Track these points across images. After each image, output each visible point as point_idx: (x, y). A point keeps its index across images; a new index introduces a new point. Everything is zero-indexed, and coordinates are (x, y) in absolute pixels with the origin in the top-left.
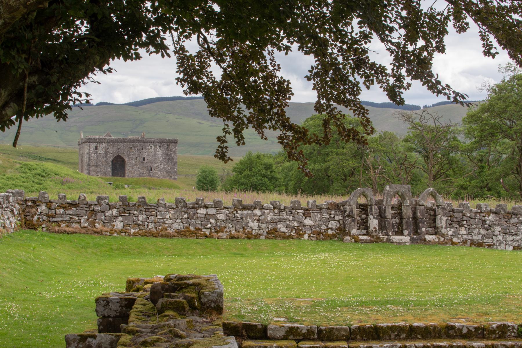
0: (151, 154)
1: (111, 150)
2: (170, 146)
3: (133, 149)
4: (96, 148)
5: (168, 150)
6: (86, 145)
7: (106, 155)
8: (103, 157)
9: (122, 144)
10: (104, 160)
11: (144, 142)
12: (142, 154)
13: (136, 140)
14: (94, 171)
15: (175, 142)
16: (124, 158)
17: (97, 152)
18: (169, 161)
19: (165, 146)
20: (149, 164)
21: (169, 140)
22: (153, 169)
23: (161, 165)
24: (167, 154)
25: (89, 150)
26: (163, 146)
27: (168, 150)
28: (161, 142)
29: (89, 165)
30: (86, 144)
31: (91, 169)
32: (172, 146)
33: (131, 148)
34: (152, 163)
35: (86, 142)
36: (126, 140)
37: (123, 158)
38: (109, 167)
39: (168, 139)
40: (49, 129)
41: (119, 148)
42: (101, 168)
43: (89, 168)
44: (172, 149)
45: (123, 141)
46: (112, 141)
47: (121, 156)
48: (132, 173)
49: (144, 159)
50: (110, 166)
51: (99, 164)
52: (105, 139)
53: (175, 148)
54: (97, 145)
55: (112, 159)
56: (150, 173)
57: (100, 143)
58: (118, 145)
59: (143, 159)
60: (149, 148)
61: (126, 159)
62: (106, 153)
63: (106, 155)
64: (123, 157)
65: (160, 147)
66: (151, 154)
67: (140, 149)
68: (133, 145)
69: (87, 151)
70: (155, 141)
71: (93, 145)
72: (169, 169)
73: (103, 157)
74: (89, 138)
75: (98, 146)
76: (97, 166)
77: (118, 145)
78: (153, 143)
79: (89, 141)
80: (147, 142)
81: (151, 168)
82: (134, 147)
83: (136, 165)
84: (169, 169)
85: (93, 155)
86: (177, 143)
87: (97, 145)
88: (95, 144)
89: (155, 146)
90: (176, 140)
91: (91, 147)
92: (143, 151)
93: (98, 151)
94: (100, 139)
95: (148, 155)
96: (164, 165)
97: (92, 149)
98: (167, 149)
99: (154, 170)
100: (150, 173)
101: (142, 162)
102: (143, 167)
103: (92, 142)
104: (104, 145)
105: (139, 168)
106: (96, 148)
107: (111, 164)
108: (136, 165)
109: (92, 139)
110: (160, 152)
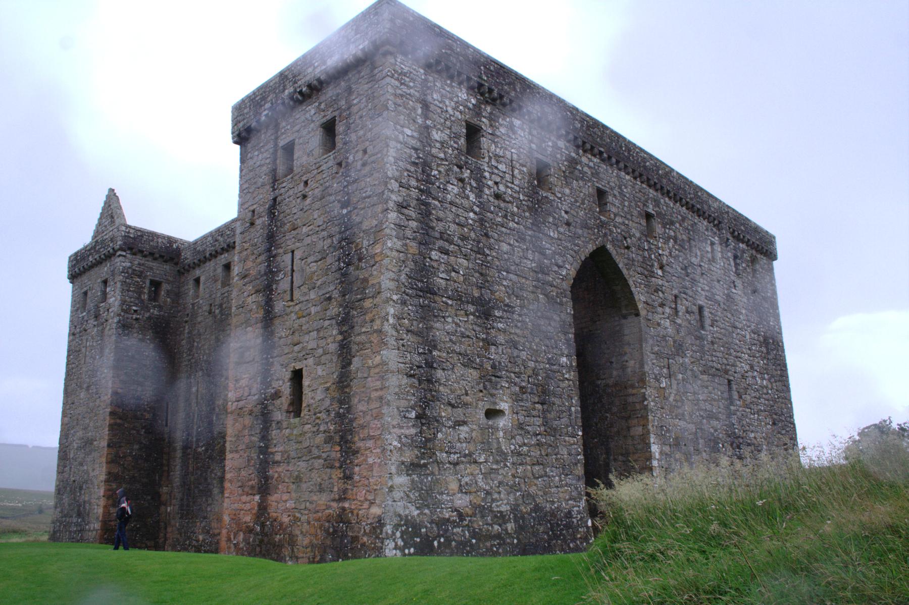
14: (468, 364)
16: (631, 283)
29: (429, 291)
31: (442, 329)
36: (629, 151)
43: (427, 314)
49: (701, 309)
54: (477, 111)
55: (570, 269)
58: (596, 174)
61: (640, 297)
76: (485, 311)
80: (700, 213)
85: (453, 189)
97: (446, 138)
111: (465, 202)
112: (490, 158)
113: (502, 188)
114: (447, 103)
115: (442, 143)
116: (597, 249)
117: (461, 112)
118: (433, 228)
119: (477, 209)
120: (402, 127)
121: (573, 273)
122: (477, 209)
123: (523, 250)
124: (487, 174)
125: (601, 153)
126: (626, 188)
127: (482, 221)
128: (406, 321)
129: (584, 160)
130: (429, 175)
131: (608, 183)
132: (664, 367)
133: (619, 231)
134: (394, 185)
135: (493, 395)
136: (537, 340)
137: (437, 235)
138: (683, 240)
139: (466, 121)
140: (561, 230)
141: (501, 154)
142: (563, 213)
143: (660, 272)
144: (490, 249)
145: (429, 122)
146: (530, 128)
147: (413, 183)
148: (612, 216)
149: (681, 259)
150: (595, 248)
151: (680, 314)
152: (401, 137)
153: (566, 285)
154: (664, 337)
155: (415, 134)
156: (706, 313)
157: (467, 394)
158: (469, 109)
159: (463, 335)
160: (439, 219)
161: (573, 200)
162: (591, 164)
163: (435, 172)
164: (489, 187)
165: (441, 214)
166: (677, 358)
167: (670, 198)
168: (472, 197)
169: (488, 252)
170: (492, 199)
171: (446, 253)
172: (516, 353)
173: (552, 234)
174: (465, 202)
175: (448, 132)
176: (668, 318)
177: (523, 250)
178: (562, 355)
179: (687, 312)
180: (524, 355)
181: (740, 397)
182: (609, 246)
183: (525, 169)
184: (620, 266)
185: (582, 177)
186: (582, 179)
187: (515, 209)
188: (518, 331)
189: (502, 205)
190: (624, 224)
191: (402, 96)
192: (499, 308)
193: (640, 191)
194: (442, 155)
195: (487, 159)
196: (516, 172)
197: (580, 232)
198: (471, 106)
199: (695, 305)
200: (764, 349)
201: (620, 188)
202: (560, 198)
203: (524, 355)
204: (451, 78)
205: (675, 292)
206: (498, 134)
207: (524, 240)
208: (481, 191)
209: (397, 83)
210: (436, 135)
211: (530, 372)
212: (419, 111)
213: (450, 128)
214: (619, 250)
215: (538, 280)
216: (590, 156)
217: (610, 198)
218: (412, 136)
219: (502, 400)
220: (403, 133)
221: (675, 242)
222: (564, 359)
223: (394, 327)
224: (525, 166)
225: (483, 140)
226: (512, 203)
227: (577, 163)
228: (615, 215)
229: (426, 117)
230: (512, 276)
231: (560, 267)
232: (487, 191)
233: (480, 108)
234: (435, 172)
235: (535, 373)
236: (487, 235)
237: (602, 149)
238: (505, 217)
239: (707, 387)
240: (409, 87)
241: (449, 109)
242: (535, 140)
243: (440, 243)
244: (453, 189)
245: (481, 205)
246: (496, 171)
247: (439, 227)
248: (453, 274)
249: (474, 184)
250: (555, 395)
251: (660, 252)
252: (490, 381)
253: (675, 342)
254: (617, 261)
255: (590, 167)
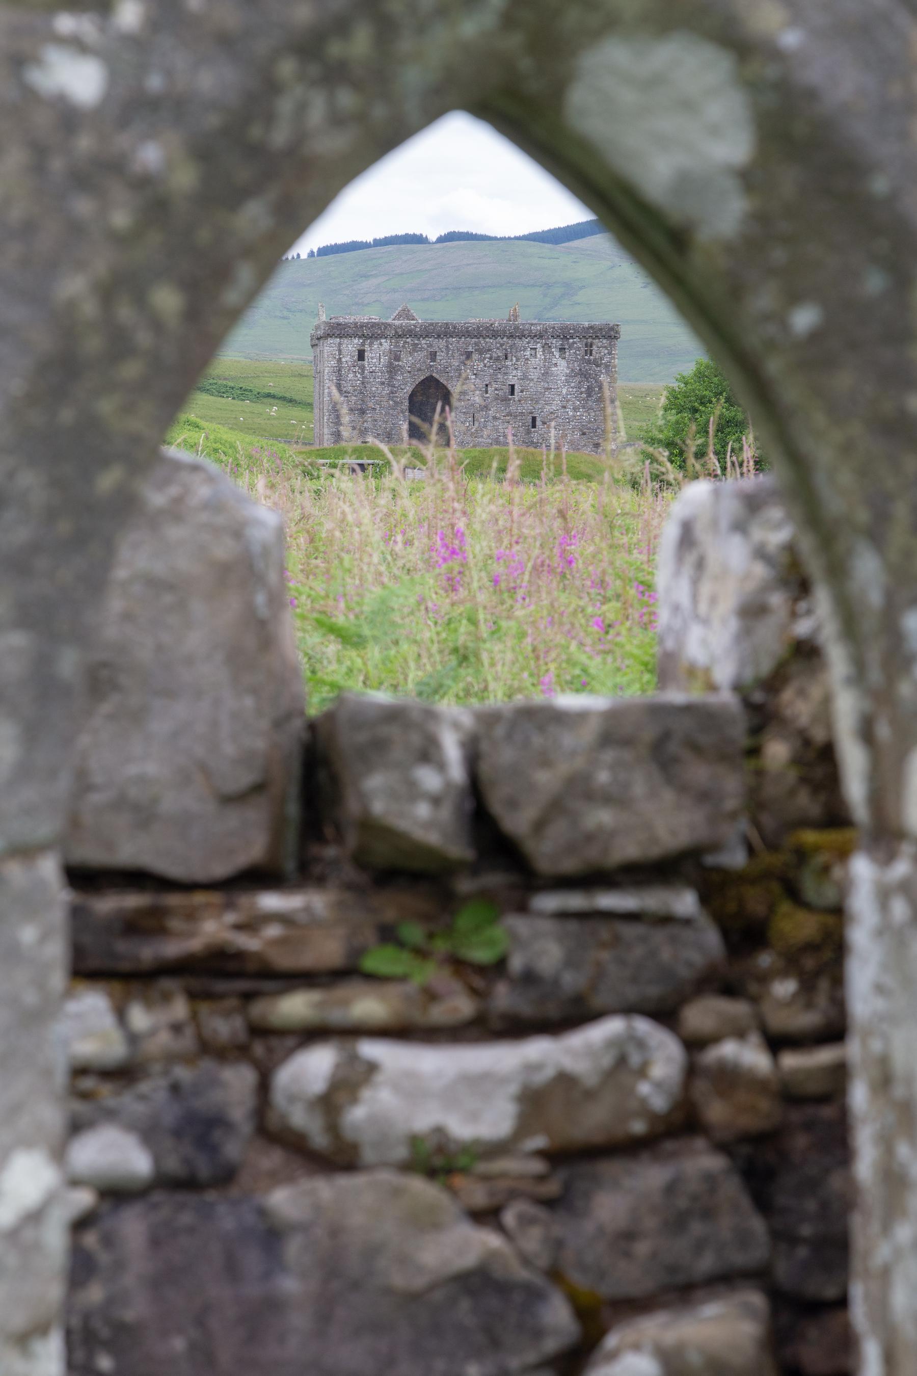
0: (534, 375)
1: (407, 361)
2: (594, 347)
3: (475, 356)
4: (361, 355)
5: (589, 362)
6: (329, 347)
7: (391, 378)
8: (383, 383)
9: (442, 343)
10: (387, 391)
11: (511, 336)
12: (506, 374)
13: (487, 329)
15: (610, 333)
17: (363, 368)
18: (589, 395)
19: (579, 349)
20: (527, 406)
21: (591, 327)
22: (538, 423)
23: (564, 407)
24: (584, 375)
25: (340, 360)
26: (571, 347)
27: (589, 362)
28: (565, 335)
30: (330, 341)
32: (599, 348)
33: (469, 355)
34: (537, 402)
35: (328, 336)
36: (455, 328)
37: (444, 387)
38: (401, 417)
39: (586, 324)
40: (301, 311)
41: (433, 356)
42: (377, 417)
44: (601, 359)
45: (446, 332)
46: (410, 331)
47: (437, 381)
48: (472, 434)
49: (513, 386)
50: (402, 412)
51: (371, 405)
52: (387, 326)
53: (610, 353)
54: (363, 344)
55: (409, 389)
56: (528, 432)
57: (374, 337)
59: (507, 389)
60: (528, 353)
62: (392, 370)
63: (391, 378)
64: (445, 383)
65: (562, 350)
66: (534, 375)
67: (498, 359)
68: (475, 343)
69: (333, 363)
70: (546, 331)
71: (351, 346)
72: (590, 422)
73: (383, 383)
74: (339, 324)
75: (367, 348)
77: (430, 346)
78: (541, 337)
79: (337, 331)
81: (534, 419)
82: (481, 352)
83: (486, 408)
84: (590, 422)
85: (351, 375)
86: (616, 338)
87: (363, 344)
88: (356, 341)
89: (547, 347)
90: (612, 329)
91: (344, 352)
92: (508, 363)
93: (366, 363)
94: (374, 325)
95: (525, 377)
96: (575, 409)
97: (348, 359)
98: (583, 358)
99: (544, 423)
100: (528, 432)
101: (505, 400)
102: (509, 414)
103: (349, 336)
104: (386, 344)
105: (495, 418)
106: (361, 355)
107: (407, 404)
108: (486, 408)
109: (346, 325)
110: (561, 367)
111: (356, 379)
112: (368, 359)
113: (374, 368)
114: (349, 346)
115: (346, 361)
116: (426, 378)
117: (355, 348)
118: (342, 391)
119: (361, 379)
120: (330, 361)
121: (411, 390)
122: (361, 379)
123: (383, 388)
124: (366, 366)
125: (434, 336)
126: (451, 344)
127: (363, 383)
128: (331, 420)
129: (424, 342)
130: (341, 374)
131: (439, 347)
132: (469, 417)
133: (443, 366)
134: (327, 381)
135: (364, 437)
136: (387, 418)
137: (343, 392)
138: (499, 356)
139: (358, 350)
140: (405, 375)
141: (374, 355)
142: (407, 368)
143: (474, 377)
144: (366, 391)
145: (341, 356)
146: (391, 340)
147: (335, 378)
148: (439, 361)
149: (494, 366)
150: (425, 377)
151: (489, 392)
152: (330, 365)
153: (407, 396)
154: (472, 405)
155: (336, 362)
156: (516, 387)
157: (353, 438)
158: (359, 345)
159: (353, 421)
160: (344, 387)
161: (413, 361)
162: (428, 342)
163: (343, 372)
164: (368, 370)
165: (345, 385)
166: (481, 412)
167: (490, 338)
168: (359, 376)
169: (365, 392)
170: (368, 374)
171: (347, 397)
172: (376, 423)
173: (399, 378)
174: (356, 379)
175: (349, 356)
176: (478, 396)
177: (383, 388)
178: (400, 421)
179: (496, 390)
180: (380, 423)
181: (544, 423)
182: (434, 375)
183: (387, 357)
184: (441, 381)
185: (421, 349)
186: (420, 351)
187: (380, 374)
188: (378, 416)
189: (374, 374)
190: (447, 362)
191: (330, 351)
192: (369, 410)
193: (464, 343)
194: (346, 366)
195: (367, 360)
196: (381, 360)
197: (416, 373)
198: (360, 343)
199: (504, 385)
200: (584, 395)
201: (447, 346)
202: (406, 363)
203: (380, 423)
204: (351, 337)
205: (487, 382)
206: (373, 348)
207: (384, 384)
208: (364, 372)
209: (329, 348)
210: (343, 360)
211: (383, 428)
212: (337, 354)
213: (350, 355)
214: (441, 375)
215: (390, 397)
216: (427, 339)
217: (438, 354)
218: (334, 363)
219: (369, 438)
220: (330, 364)
221: (491, 358)
222: (402, 422)
223: (327, 422)
224: (387, 356)
225: (366, 353)
226: (378, 372)
227: (418, 345)
228: (441, 360)
229: (340, 355)
230: (376, 398)
231: (402, 389)
232: (366, 372)
233: (364, 342)
234: (343, 372)
235: (386, 428)
236: (365, 387)
237: (434, 334)
238: (375, 378)
239: (509, 422)
240: (333, 347)
241: (350, 349)
242: (393, 344)
243: (345, 394)
244: (351, 375)
245: (363, 378)
246: (371, 363)
247: (345, 389)
248: (350, 403)
249: (360, 371)
250: (395, 435)
251: (475, 367)
252: (364, 433)
253: (480, 406)
254: (439, 380)
255: (426, 344)
